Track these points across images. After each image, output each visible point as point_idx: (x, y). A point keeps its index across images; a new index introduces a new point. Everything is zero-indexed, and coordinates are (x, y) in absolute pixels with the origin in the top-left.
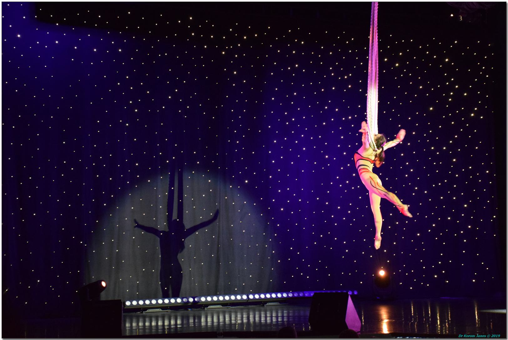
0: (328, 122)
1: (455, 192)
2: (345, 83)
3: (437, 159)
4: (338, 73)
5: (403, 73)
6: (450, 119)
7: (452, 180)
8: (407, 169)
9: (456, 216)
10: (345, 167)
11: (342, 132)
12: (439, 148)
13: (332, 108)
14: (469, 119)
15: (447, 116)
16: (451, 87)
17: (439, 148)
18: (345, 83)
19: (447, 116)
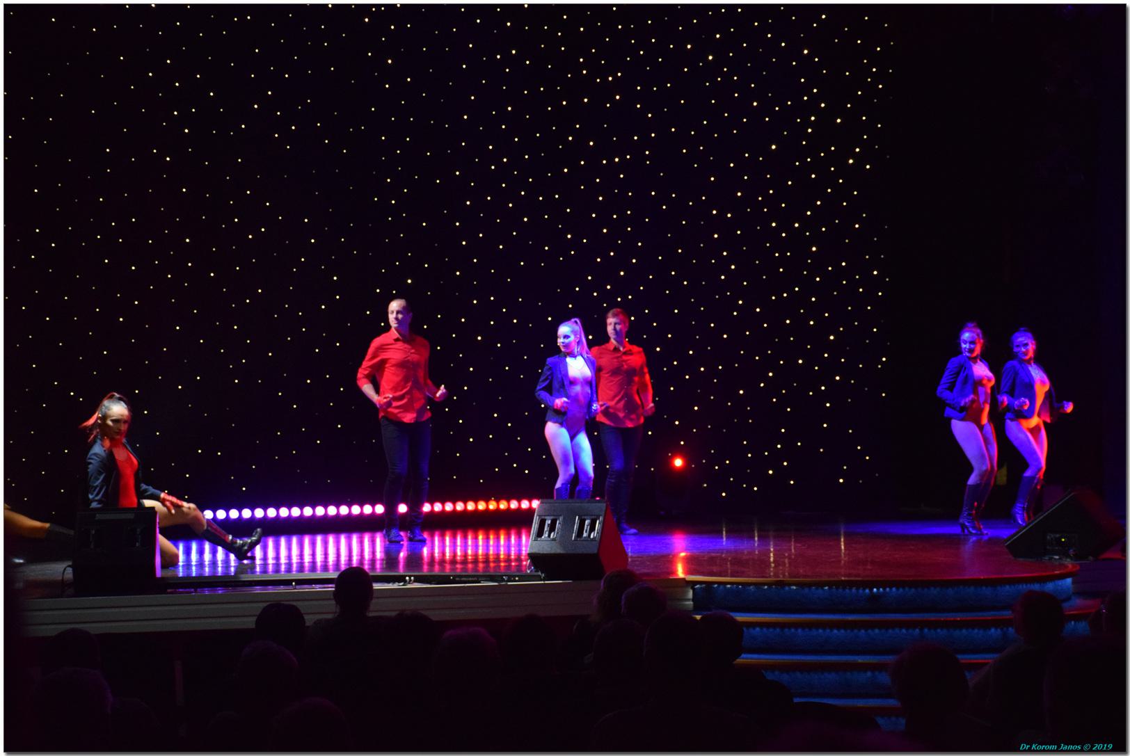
0: (574, 167)
1: (814, 311)
2: (609, 90)
3: (781, 245)
4: (595, 70)
5: (722, 74)
6: (809, 168)
7: (810, 287)
8: (723, 265)
9: (812, 358)
10: (605, 256)
11: (599, 190)
12: (785, 225)
13: (581, 137)
14: (843, 169)
15: (803, 162)
16: (812, 107)
17: (785, 225)
18: (609, 90)
19: (803, 162)
